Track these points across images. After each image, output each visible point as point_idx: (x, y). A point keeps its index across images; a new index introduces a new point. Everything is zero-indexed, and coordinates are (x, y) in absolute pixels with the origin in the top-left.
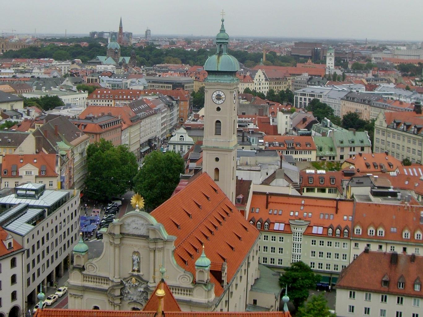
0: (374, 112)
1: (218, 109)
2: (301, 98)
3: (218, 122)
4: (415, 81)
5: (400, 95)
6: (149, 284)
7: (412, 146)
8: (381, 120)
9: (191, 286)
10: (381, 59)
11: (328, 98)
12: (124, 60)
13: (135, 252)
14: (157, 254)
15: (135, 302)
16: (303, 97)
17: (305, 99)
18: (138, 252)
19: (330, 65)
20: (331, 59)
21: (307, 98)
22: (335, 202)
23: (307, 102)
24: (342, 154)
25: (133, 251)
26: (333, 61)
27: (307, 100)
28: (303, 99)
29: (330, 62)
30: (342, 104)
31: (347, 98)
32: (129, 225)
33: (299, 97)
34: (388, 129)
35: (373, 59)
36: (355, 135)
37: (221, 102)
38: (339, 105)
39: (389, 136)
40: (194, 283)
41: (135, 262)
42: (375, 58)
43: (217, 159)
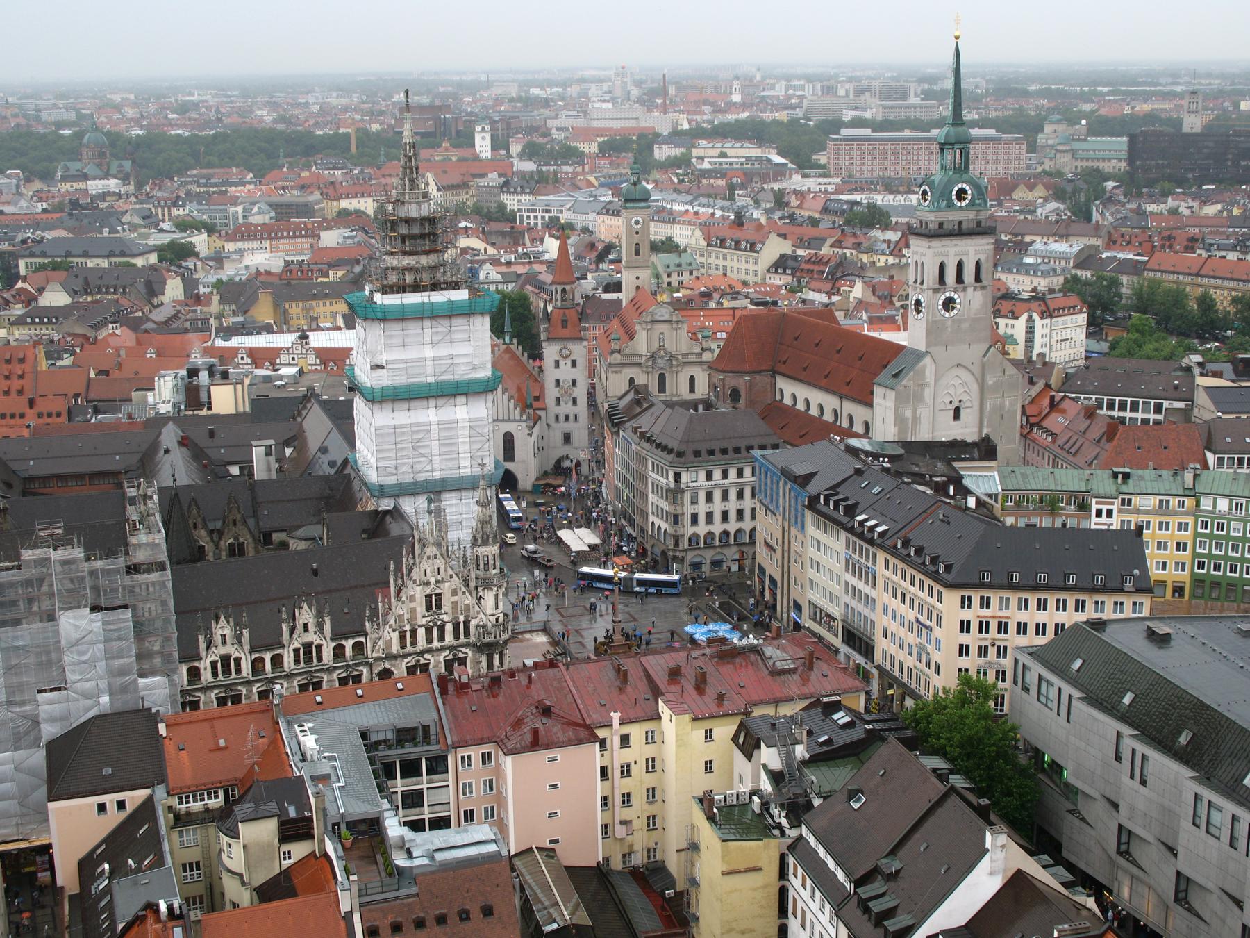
1: (637, 233)
2: (529, 218)
3: (637, 244)
4: (677, 175)
5: (672, 201)
7: (744, 266)
10: (568, 129)
12: (121, 166)
15: (662, 368)
16: (532, 215)
17: (536, 218)
19: (484, 149)
20: (484, 138)
21: (540, 215)
23: (540, 222)
24: (669, 280)
26: (488, 141)
27: (539, 218)
28: (532, 218)
29: (484, 143)
31: (608, 211)
33: (525, 215)
35: (554, 131)
37: (639, 226)
39: (711, 257)
40: (702, 349)
42: (558, 129)
43: (638, 278)
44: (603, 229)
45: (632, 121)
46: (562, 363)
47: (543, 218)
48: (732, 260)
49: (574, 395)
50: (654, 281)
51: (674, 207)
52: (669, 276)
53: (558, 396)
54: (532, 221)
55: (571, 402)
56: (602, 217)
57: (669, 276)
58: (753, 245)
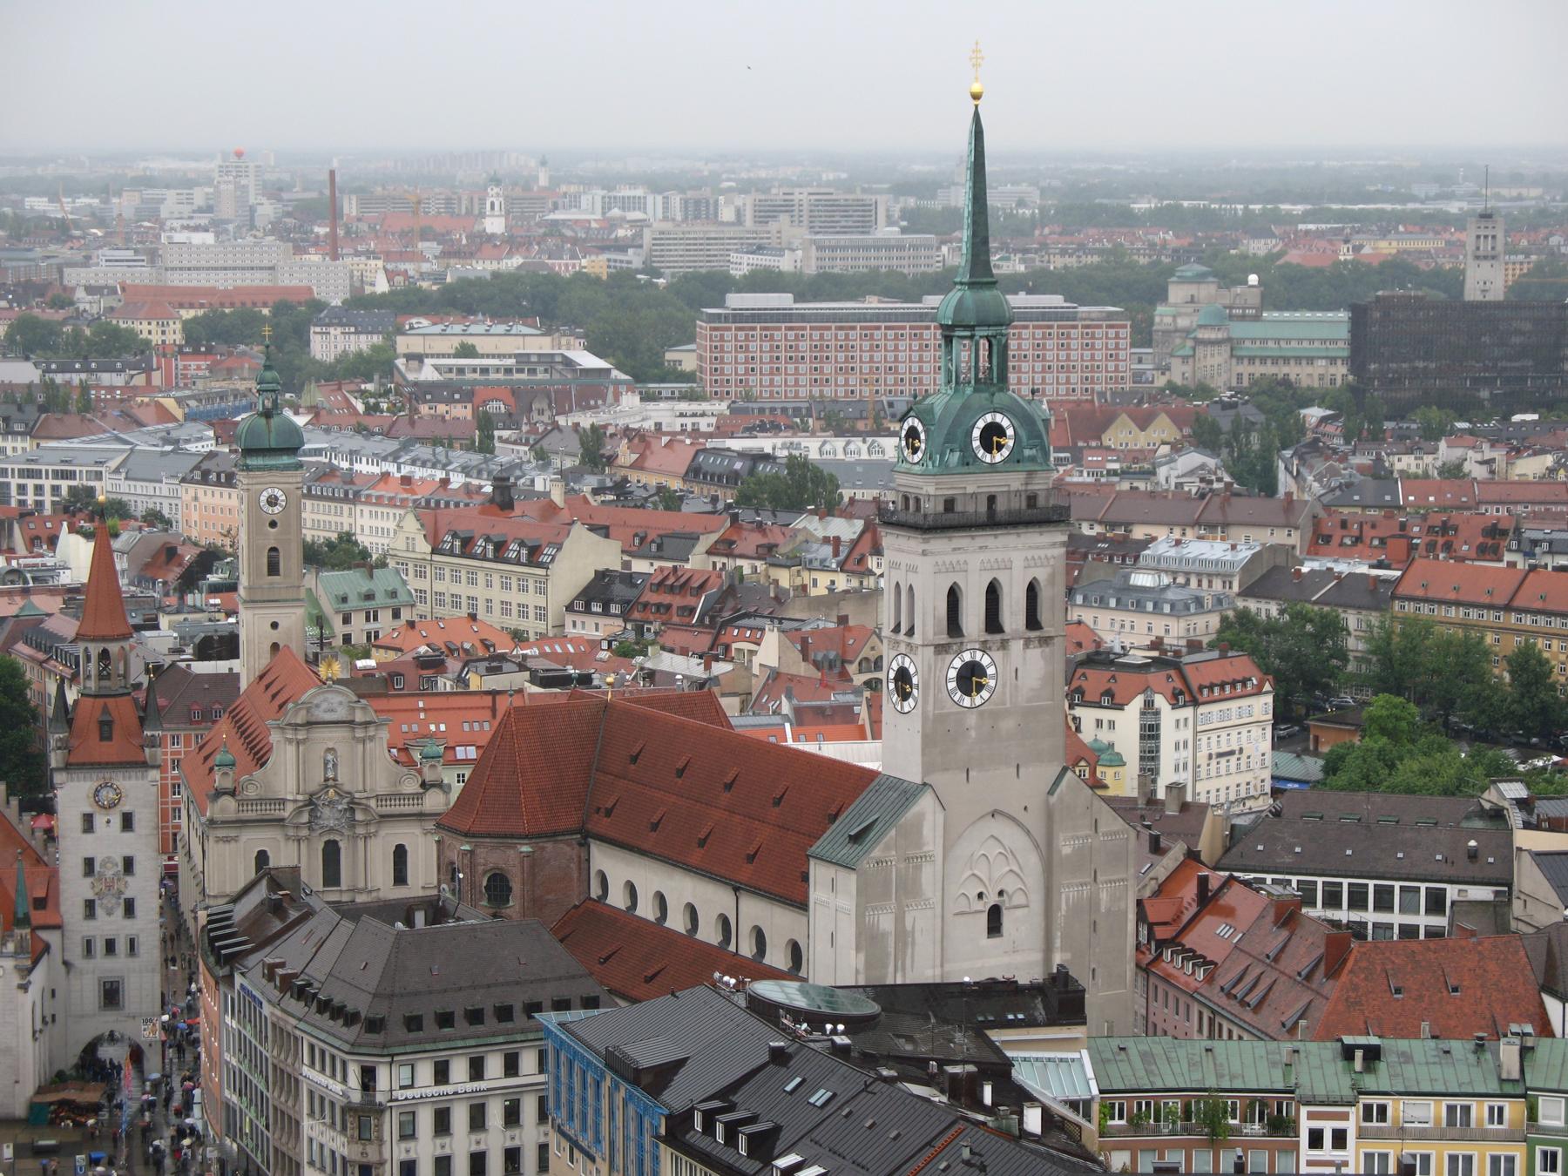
0: (316, 517)
1: (273, 524)
2: (22, 489)
3: (274, 549)
4: (363, 394)
5: (352, 453)
6: (357, 795)
7: (515, 597)
8: (411, 536)
9: (421, 791)
10: (113, 291)
11: (126, 479)
13: (329, 750)
14: (368, 745)
15: (331, 830)
16: (30, 483)
17: (39, 490)
18: (332, 749)
21: (47, 483)
22: (490, 698)
23: (48, 498)
24: (347, 629)
25: (325, 747)
27: (47, 490)
28: (30, 490)
30: (187, 497)
32: (317, 706)
33: (14, 482)
34: (436, 558)
35: (80, 294)
36: (371, 576)
37: (277, 509)
38: (173, 502)
39: (441, 578)
40: (423, 785)
41: (330, 766)
42: (90, 290)
43: (275, 625)
44: (195, 516)
45: (258, 274)
46: (99, 820)
47: (56, 490)
48: (489, 584)
49: (128, 894)
50: (313, 631)
51: (357, 467)
52: (346, 620)
53: (90, 895)
54: (30, 498)
55: (120, 911)
56: (192, 488)
57: (346, 620)
58: (534, 551)
